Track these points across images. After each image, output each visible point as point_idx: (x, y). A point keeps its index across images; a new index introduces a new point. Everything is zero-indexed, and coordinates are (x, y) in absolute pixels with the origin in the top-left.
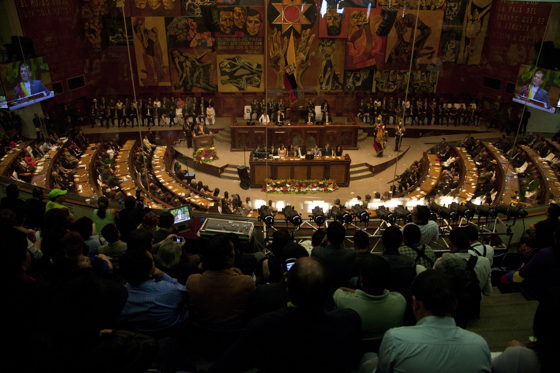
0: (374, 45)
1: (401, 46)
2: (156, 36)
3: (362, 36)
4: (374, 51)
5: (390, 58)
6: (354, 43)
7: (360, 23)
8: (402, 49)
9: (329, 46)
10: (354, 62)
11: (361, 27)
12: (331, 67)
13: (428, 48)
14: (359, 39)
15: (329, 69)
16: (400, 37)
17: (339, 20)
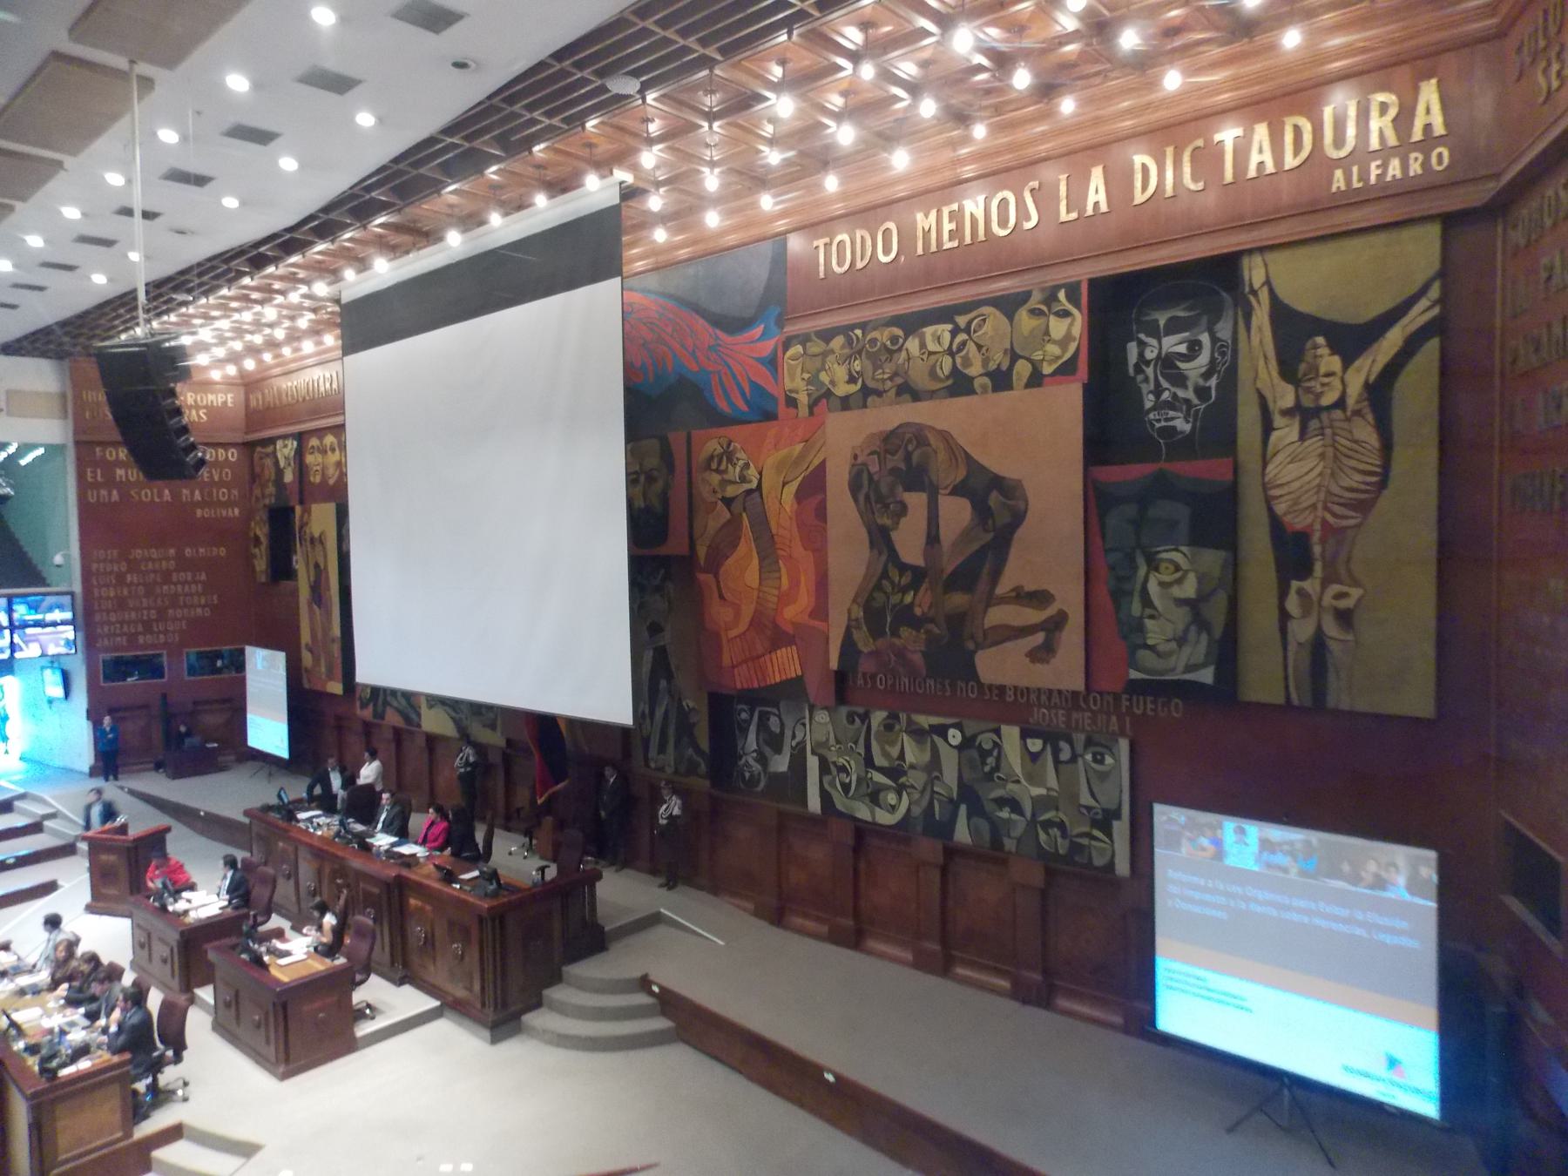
0: (785, 582)
1: (889, 589)
2: (325, 557)
3: (742, 548)
4: (790, 612)
5: (848, 646)
6: (716, 576)
7: (731, 491)
8: (895, 599)
9: (658, 589)
10: (726, 661)
11: (737, 507)
12: (670, 677)
13: (1023, 597)
14: (730, 561)
15: (663, 684)
16: (881, 538)
17: (659, 485)
